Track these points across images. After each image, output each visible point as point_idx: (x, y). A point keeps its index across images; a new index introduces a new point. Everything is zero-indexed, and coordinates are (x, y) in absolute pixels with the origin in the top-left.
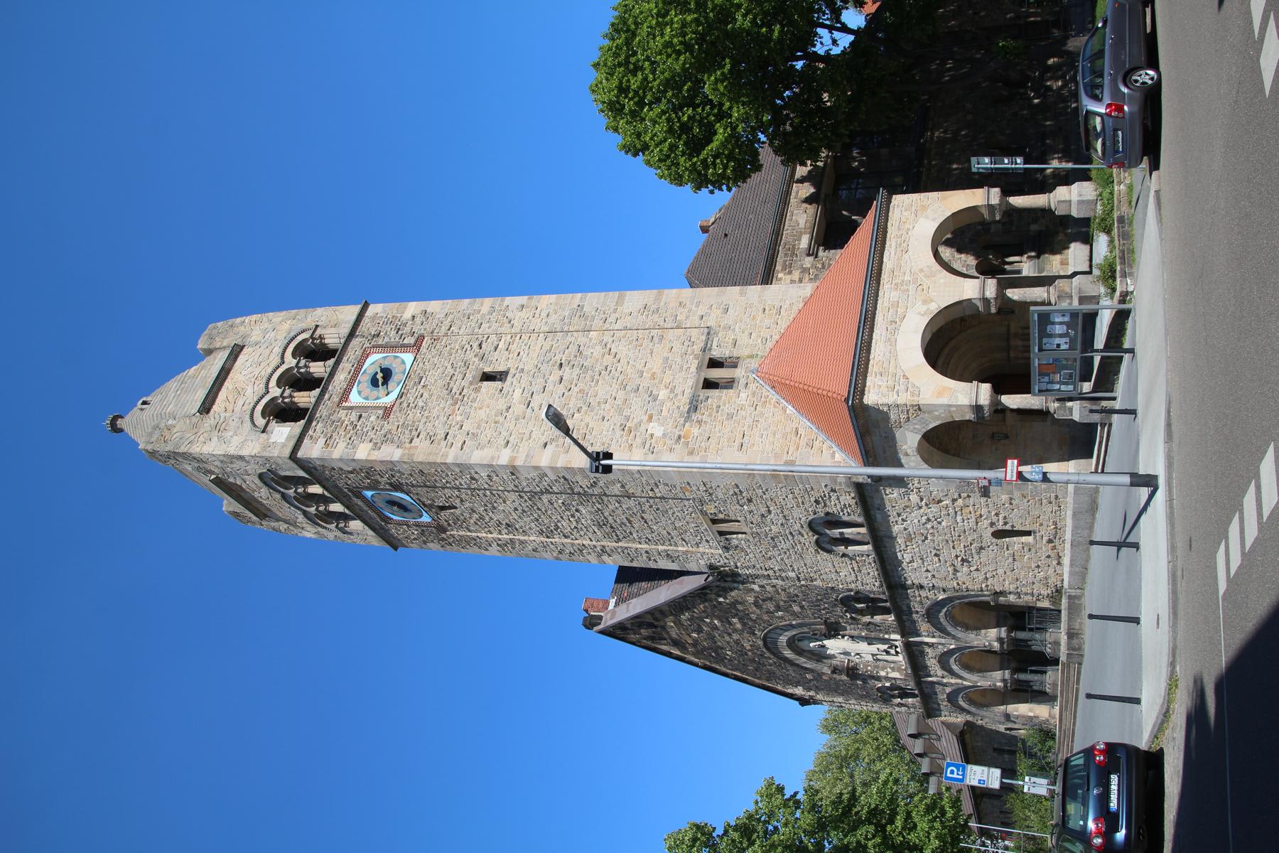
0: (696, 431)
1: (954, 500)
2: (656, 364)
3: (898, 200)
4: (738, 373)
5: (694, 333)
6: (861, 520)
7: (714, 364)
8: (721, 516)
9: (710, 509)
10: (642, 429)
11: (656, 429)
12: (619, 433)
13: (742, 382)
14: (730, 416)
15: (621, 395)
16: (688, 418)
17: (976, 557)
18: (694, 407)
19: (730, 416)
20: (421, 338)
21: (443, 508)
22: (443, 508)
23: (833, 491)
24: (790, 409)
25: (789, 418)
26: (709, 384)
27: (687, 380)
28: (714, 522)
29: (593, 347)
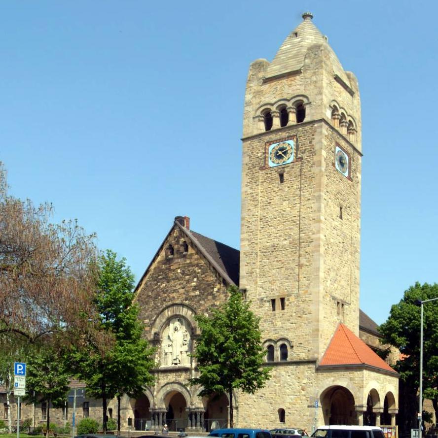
0: (328, 299)
1: (305, 395)
2: (343, 283)
3: (398, 380)
4: (341, 316)
5: (349, 298)
6: (289, 359)
7: (343, 305)
8: (286, 302)
9: (292, 299)
10: (328, 278)
11: (329, 283)
12: (328, 267)
13: (338, 317)
14: (331, 313)
15: (336, 268)
16: (331, 296)
17: (265, 401)
18: (334, 298)
19: (331, 313)
20: (352, 181)
21: (281, 176)
22: (281, 176)
23: (309, 351)
24: (332, 336)
25: (331, 336)
26: (338, 303)
27: (340, 297)
28: (283, 300)
29: (347, 256)
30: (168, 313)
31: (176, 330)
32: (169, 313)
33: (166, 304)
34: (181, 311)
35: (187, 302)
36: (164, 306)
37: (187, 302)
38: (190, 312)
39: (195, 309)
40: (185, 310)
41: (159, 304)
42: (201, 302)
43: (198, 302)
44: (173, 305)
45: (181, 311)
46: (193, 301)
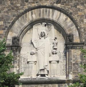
30: (32, 16)
31: (43, 35)
32: (34, 16)
33: (29, 5)
34: (51, 14)
35: (59, 5)
36: (26, 7)
37: (59, 5)
38: (63, 17)
39: (71, 13)
40: (57, 13)
41: (19, 5)
42: (78, 7)
43: (75, 6)
44: (40, 7)
45: (51, 14)
46: (67, 5)
